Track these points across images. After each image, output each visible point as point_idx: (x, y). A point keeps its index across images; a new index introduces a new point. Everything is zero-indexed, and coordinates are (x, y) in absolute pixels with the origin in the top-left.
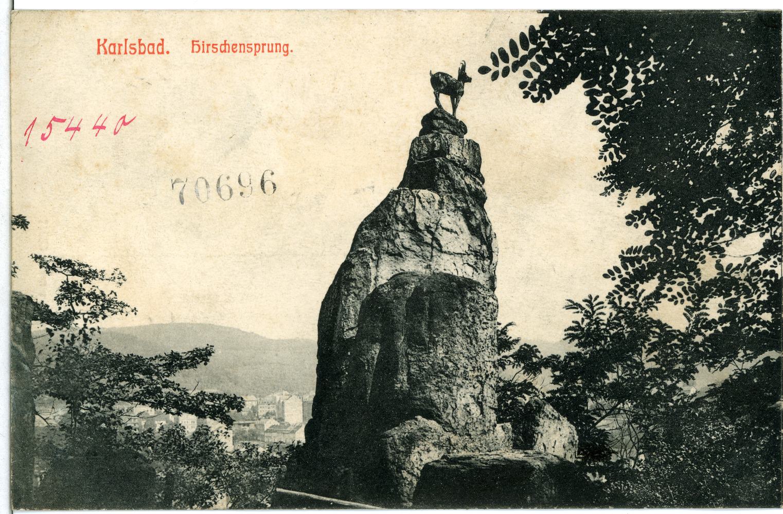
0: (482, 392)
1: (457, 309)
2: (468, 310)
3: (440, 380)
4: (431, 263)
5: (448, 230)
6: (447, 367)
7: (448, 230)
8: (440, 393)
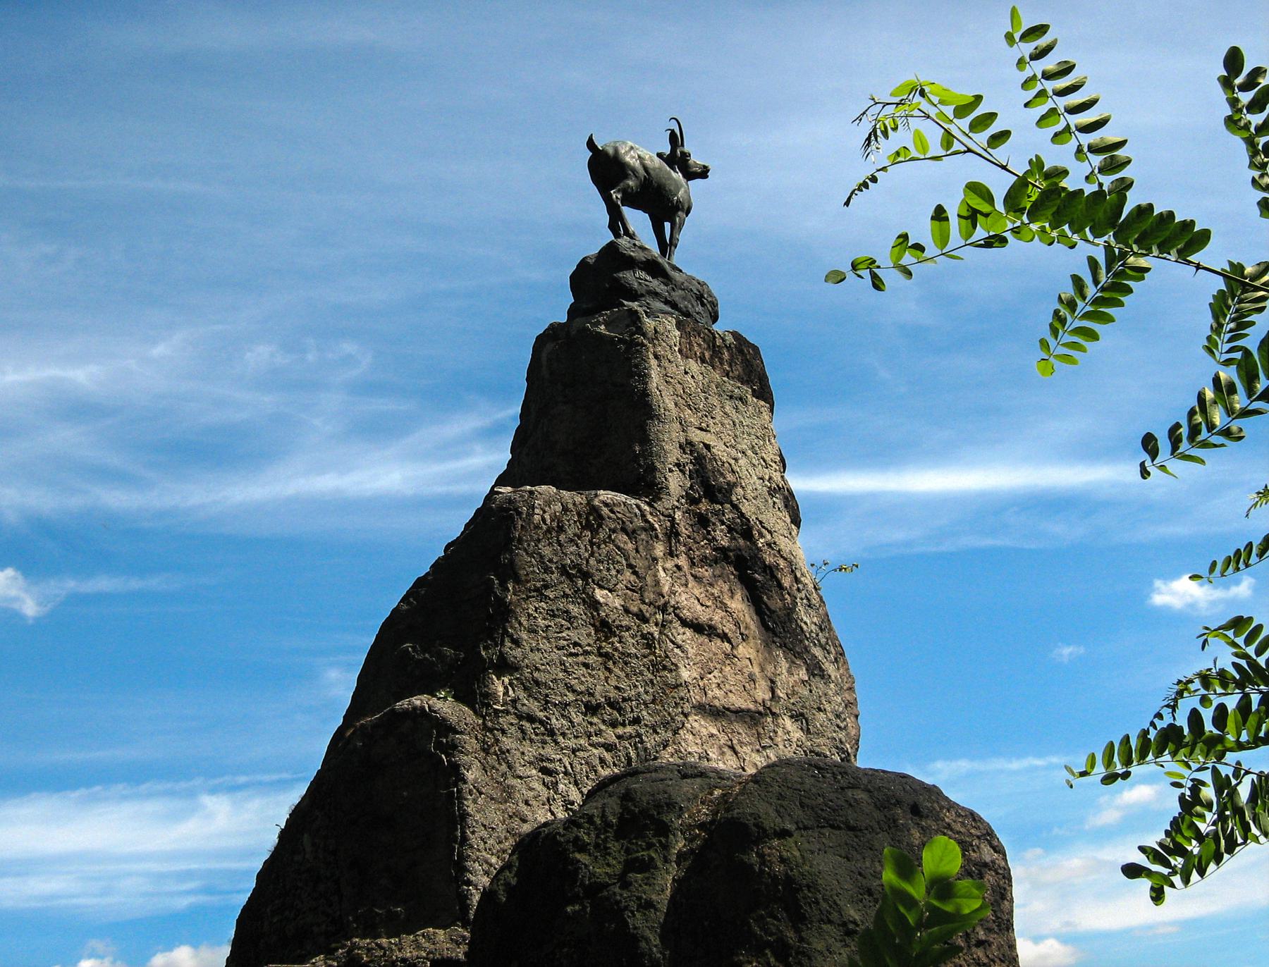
5: (698, 627)
7: (698, 627)
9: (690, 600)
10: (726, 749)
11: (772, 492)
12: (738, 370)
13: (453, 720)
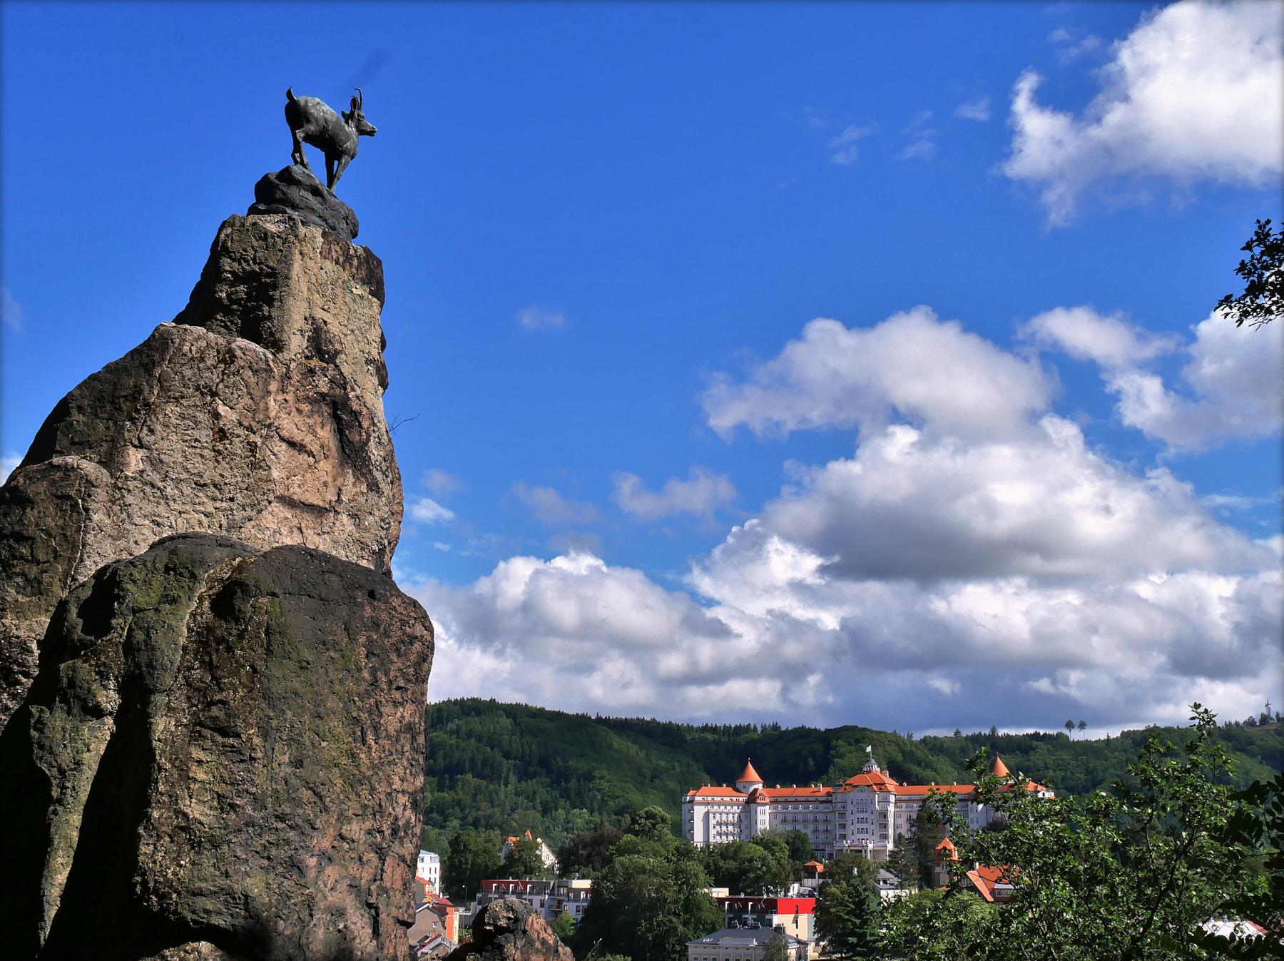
0: (378, 877)
2: (363, 651)
3: (273, 838)
5: (292, 444)
6: (297, 803)
7: (292, 444)
8: (272, 875)
9: (290, 425)
10: (294, 529)
11: (368, 362)
12: (363, 273)
13: (92, 477)
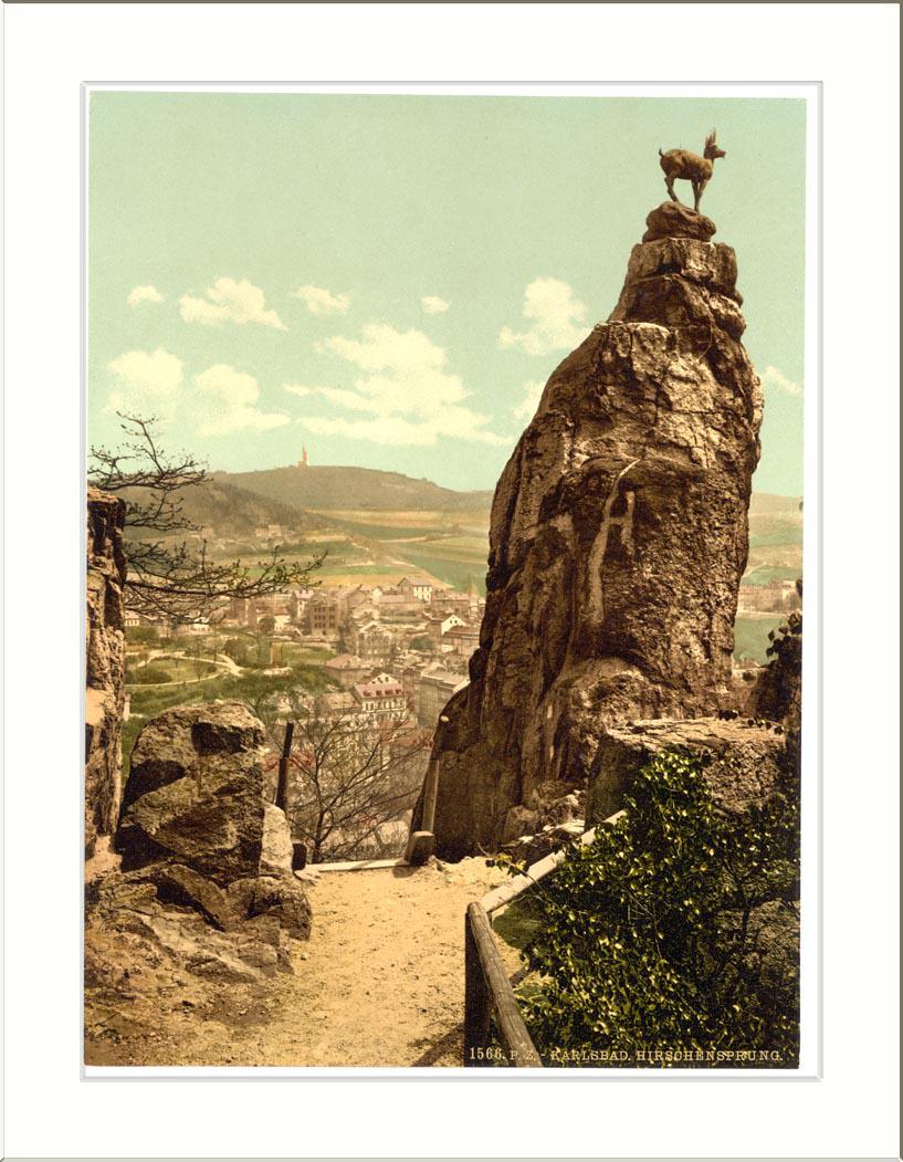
1: (675, 511)
4: (654, 428)
5: (680, 379)
7: (680, 379)
